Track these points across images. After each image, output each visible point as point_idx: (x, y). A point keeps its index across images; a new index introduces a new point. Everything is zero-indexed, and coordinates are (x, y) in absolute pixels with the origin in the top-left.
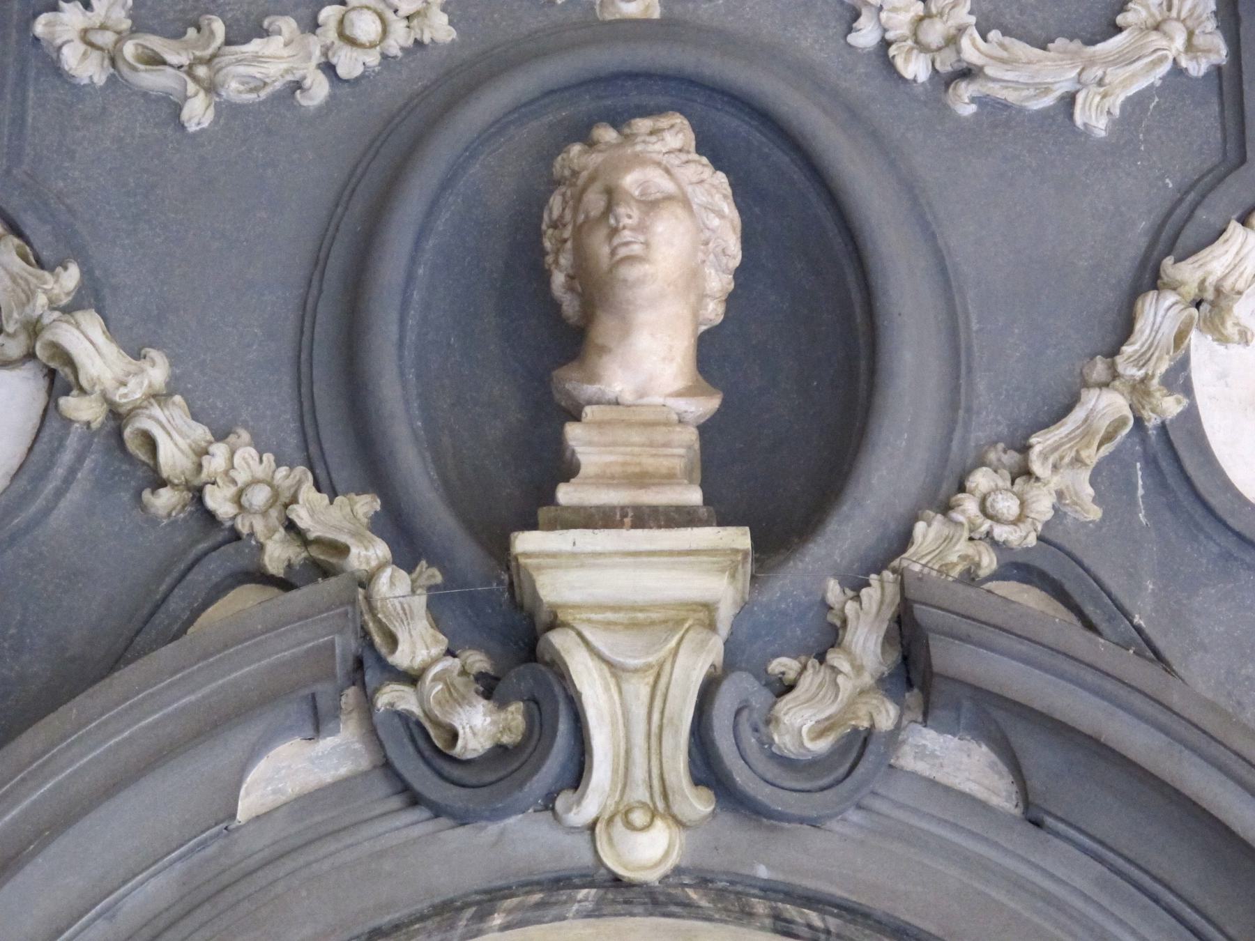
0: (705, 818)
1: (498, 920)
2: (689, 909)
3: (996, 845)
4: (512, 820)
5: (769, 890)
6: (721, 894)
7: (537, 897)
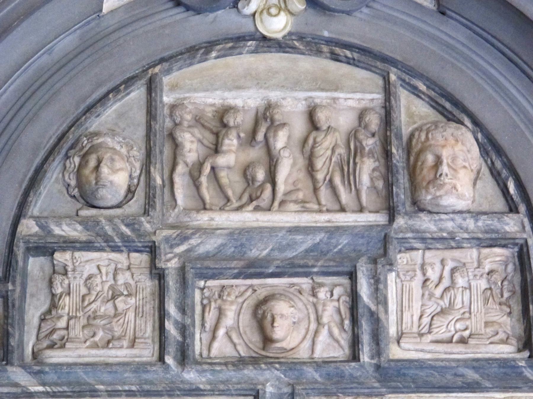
0: (302, 11)
1: (214, 54)
2: (294, 50)
3: (425, 22)
4: (220, 12)
5: (329, 42)
6: (308, 44)
7: (230, 45)
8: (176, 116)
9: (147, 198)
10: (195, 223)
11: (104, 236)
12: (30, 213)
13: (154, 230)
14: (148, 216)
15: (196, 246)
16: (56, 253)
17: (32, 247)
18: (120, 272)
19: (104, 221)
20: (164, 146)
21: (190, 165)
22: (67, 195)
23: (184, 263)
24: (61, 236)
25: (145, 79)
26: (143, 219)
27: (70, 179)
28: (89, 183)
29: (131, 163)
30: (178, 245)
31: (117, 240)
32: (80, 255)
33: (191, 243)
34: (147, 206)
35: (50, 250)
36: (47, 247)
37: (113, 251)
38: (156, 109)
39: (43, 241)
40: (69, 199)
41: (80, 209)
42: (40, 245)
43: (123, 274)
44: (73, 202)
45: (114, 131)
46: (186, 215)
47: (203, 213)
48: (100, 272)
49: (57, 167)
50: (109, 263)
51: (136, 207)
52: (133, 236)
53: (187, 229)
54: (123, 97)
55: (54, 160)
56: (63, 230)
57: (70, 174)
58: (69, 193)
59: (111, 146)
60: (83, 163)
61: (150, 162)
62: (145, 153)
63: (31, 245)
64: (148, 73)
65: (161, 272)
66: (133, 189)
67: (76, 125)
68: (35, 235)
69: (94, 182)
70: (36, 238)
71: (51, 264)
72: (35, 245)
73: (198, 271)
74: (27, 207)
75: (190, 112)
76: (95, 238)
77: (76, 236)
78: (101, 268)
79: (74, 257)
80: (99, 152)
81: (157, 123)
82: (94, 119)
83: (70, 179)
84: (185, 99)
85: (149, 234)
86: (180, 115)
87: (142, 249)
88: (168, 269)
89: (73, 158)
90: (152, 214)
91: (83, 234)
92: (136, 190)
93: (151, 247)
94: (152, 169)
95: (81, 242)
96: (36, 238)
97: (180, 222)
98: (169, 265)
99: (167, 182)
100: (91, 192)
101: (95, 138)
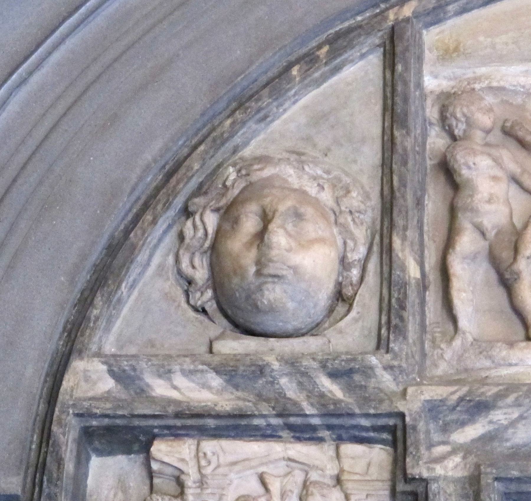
8: (456, 118)
9: (384, 313)
10: (504, 372)
11: (277, 400)
12: (94, 348)
13: (401, 388)
14: (387, 352)
15: (506, 428)
16: (155, 443)
17: (98, 427)
18: (315, 491)
19: (276, 365)
20: (423, 190)
21: (491, 234)
22: (184, 305)
23: (478, 466)
24: (170, 401)
25: (380, 34)
26: (373, 360)
27: (194, 267)
28: (240, 271)
29: (344, 229)
30: (463, 424)
31: (309, 410)
32: (218, 449)
33: (495, 419)
34: (384, 331)
35: (142, 438)
36: (134, 428)
37: (299, 439)
38: (406, 100)
39: (125, 412)
40: (192, 314)
41: (217, 338)
42: (118, 422)
43: (323, 496)
44: (201, 323)
45: (300, 154)
46: (481, 353)
47: (521, 349)
48: (267, 490)
49: (160, 240)
50: (288, 470)
51: (357, 334)
52: (350, 400)
53: (484, 385)
54: (324, 78)
55: (154, 222)
56: (175, 388)
57: (193, 254)
58: (192, 302)
59: (296, 186)
60: (227, 226)
61: (392, 226)
62: (379, 206)
63: (94, 423)
64: (386, 18)
65: (420, 489)
66: (348, 291)
67: (210, 139)
68: (106, 397)
69: (252, 269)
70: (108, 405)
71: (144, 474)
72: (106, 421)
73: (513, 487)
74: (88, 331)
75: (490, 110)
76: (255, 404)
77: (208, 401)
78: (269, 480)
79: (201, 454)
80: (266, 196)
81: (408, 133)
82: (254, 126)
83: (194, 267)
84: (478, 79)
85: (390, 397)
86: (464, 115)
87: (372, 434)
88: (436, 479)
89: (202, 215)
90: (396, 348)
91: (227, 396)
92: (356, 294)
93: (392, 430)
94: (397, 243)
95: (218, 416)
96: (108, 405)
97: (466, 370)
98: (439, 470)
99: (433, 277)
100: (244, 295)
101: (256, 167)
